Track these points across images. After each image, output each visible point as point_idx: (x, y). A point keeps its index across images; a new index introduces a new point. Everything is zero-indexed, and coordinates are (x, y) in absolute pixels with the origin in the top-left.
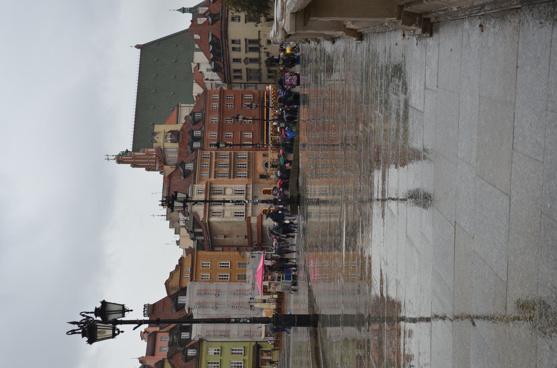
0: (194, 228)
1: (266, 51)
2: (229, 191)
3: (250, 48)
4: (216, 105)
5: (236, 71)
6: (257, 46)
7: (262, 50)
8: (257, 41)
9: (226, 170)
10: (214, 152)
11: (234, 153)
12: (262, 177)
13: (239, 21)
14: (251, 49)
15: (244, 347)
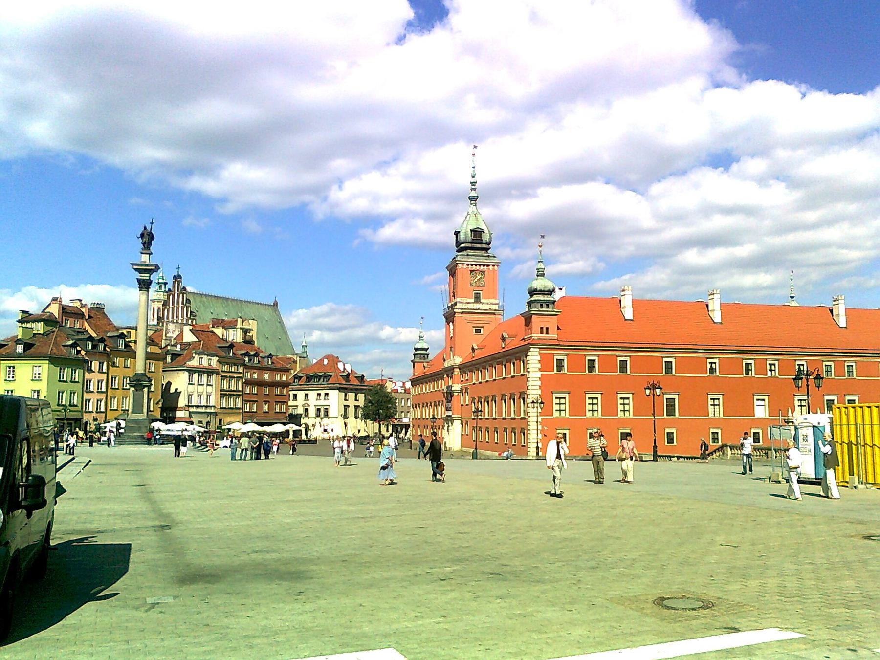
0: (172, 355)
1: (318, 425)
2: (209, 389)
3: (319, 410)
4: (278, 378)
5: (295, 396)
6: (322, 416)
7: (318, 420)
8: (326, 414)
9: (226, 387)
10: (241, 375)
11: (240, 395)
12: (220, 420)
13: (345, 400)
14: (319, 410)
15: (76, 406)
